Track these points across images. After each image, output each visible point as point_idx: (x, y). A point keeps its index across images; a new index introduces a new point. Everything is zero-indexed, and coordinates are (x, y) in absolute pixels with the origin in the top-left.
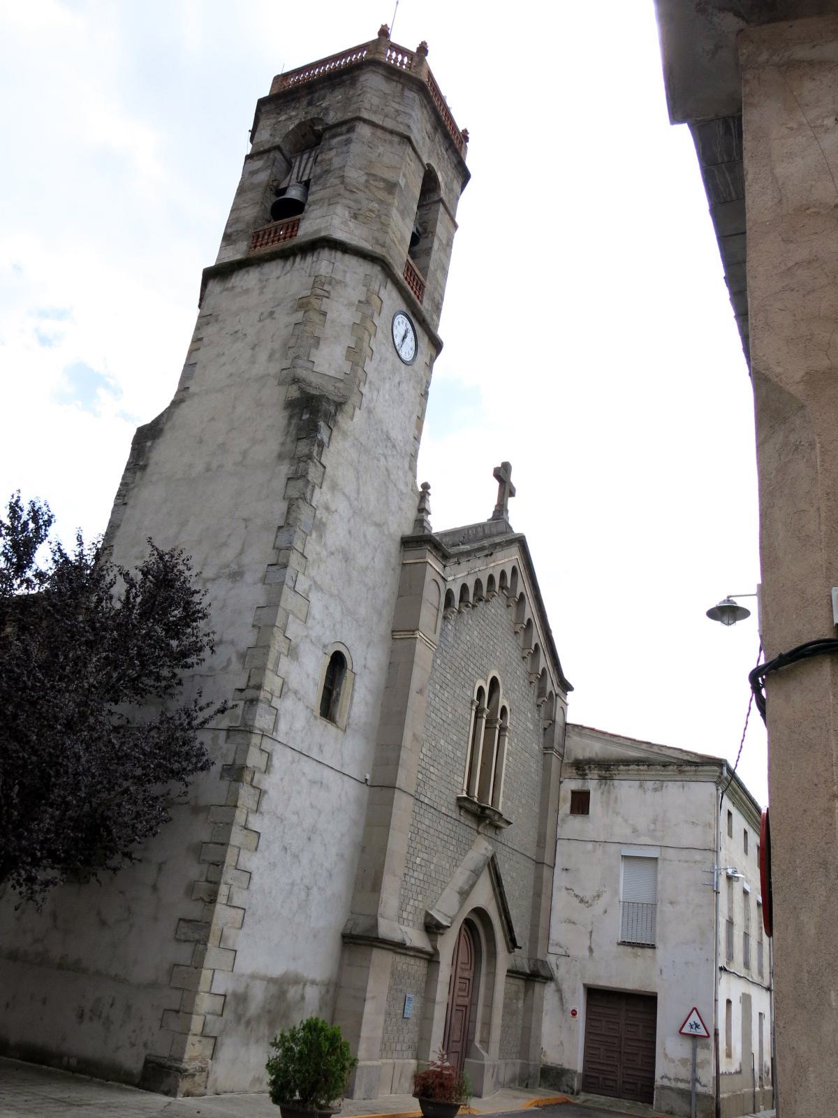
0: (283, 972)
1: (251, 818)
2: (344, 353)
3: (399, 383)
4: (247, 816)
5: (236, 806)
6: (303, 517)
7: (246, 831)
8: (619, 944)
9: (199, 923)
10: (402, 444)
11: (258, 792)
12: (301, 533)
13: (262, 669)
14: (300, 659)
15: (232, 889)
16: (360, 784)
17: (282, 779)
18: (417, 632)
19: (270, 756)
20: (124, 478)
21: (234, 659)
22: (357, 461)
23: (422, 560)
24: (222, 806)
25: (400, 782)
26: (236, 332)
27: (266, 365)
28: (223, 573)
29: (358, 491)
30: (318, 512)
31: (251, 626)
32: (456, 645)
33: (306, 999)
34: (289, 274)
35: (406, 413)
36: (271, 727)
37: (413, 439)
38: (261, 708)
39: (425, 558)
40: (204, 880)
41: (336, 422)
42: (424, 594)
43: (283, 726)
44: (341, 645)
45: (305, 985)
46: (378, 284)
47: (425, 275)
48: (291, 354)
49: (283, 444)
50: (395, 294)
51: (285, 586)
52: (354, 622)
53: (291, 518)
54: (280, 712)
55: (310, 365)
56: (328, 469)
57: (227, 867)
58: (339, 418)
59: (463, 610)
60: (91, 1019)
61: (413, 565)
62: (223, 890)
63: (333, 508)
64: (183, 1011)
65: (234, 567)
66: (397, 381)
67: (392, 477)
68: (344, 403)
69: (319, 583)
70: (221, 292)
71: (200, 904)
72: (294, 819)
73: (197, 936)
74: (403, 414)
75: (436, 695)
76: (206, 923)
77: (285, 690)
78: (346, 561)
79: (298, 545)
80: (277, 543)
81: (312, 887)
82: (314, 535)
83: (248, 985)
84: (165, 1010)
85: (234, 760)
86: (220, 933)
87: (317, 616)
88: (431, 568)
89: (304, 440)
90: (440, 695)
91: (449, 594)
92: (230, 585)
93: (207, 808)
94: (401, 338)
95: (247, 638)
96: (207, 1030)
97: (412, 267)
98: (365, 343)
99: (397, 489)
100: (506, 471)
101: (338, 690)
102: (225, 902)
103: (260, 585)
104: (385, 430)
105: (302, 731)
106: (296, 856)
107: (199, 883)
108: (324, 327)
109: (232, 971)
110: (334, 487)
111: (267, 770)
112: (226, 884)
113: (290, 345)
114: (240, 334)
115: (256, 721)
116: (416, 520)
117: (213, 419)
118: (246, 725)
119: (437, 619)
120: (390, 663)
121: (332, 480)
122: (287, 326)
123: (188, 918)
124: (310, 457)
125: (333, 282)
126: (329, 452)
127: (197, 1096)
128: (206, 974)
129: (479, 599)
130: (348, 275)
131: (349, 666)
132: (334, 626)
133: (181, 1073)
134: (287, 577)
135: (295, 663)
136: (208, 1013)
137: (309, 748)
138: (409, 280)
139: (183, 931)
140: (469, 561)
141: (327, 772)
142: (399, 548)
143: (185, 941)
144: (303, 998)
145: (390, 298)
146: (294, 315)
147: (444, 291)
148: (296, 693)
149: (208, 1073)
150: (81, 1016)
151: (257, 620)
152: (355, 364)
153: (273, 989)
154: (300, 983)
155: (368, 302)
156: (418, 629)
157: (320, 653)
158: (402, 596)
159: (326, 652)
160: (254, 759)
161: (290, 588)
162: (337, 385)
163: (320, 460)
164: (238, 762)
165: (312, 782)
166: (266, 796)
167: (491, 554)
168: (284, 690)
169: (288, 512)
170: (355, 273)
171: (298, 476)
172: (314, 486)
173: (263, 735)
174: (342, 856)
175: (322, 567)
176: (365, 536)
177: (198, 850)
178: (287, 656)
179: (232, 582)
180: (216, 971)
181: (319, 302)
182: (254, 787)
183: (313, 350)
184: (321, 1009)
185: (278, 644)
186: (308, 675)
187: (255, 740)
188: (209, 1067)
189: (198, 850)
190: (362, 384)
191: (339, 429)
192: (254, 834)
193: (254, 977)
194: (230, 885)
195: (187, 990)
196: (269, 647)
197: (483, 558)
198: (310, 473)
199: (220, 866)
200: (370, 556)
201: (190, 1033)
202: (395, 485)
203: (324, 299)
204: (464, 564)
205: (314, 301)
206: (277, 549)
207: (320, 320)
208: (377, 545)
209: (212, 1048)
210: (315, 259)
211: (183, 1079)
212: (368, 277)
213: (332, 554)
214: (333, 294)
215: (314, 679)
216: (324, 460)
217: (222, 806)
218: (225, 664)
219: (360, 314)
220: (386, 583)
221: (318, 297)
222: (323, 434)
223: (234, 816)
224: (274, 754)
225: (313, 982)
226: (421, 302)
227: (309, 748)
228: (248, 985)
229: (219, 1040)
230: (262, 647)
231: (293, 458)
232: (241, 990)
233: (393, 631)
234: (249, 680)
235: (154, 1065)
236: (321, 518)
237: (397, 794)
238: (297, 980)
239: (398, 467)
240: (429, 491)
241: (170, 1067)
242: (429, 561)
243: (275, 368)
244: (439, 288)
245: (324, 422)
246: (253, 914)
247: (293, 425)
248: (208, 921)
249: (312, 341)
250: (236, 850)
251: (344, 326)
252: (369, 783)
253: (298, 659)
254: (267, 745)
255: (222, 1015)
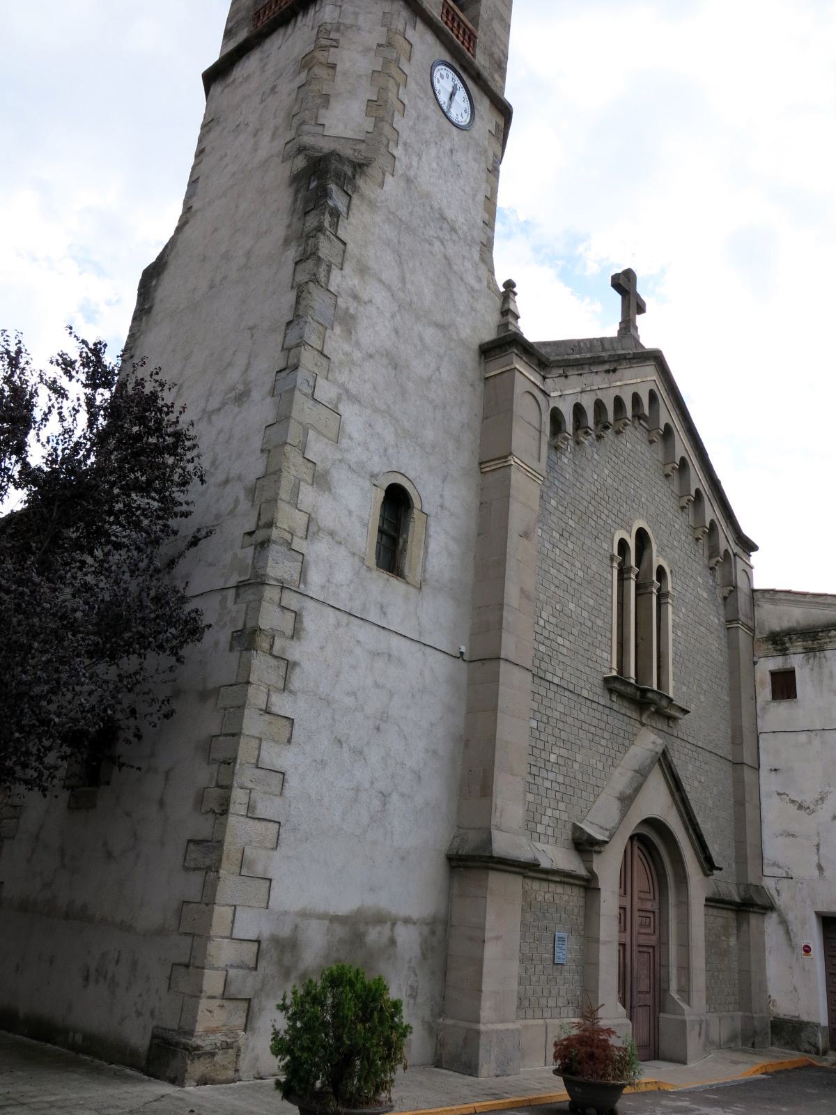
0: (355, 908)
1: (275, 698)
2: (364, 108)
3: (451, 151)
4: (268, 695)
5: (248, 683)
6: (316, 305)
7: (267, 717)
8: (415, 29)
9: (210, 844)
10: (465, 228)
11: (283, 664)
12: (315, 325)
13: (273, 501)
14: (333, 490)
15: (252, 795)
16: (453, 658)
17: (322, 648)
18: (510, 458)
19: (298, 616)
20: (131, 330)
21: (242, 497)
22: (396, 241)
23: (508, 368)
24: (231, 685)
25: (508, 649)
26: (238, 126)
27: (270, 146)
28: (229, 399)
29: (403, 280)
30: (340, 300)
31: (259, 451)
32: (578, 484)
33: (399, 943)
34: (290, 38)
35: (467, 189)
36: (296, 577)
37: (482, 224)
38: (275, 551)
39: (512, 363)
40: (213, 784)
41: (356, 188)
42: (514, 409)
43: (315, 577)
44: (399, 475)
45: (394, 924)
46: (403, 22)
47: (476, 25)
48: (295, 122)
49: (289, 226)
50: (430, 38)
51: (297, 393)
52: (418, 448)
53: (301, 307)
54: (307, 558)
55: (319, 129)
56: (350, 246)
57: (241, 764)
58: (360, 182)
59: (582, 439)
60: (97, 981)
61: (498, 377)
62: (238, 796)
63: (366, 297)
64: (193, 965)
65: (241, 387)
66: (448, 146)
67: (455, 267)
68: (367, 165)
69: (354, 393)
70: (222, 91)
71: (211, 817)
72: (349, 701)
73: (208, 862)
74: (463, 191)
75: (554, 546)
76: (218, 842)
77: (313, 528)
78: (395, 368)
79: (314, 340)
80: (286, 343)
81: (390, 795)
82: (338, 329)
83: (296, 927)
84: (174, 964)
85: (245, 624)
86: (239, 856)
87: (355, 435)
88: (522, 377)
89: (313, 212)
90: (560, 545)
91: (556, 416)
92: (236, 410)
93: (217, 691)
94: (448, 96)
95: (254, 466)
96: (232, 990)
97: (453, 10)
98: (390, 94)
99: (465, 284)
100: (629, 281)
101: (405, 536)
102: (244, 813)
103: (269, 399)
104: (436, 206)
105: (348, 586)
106: (359, 752)
107: (209, 790)
108: (334, 81)
109: (267, 908)
110: (363, 270)
111: (296, 634)
112: (241, 788)
113: (294, 113)
114: (242, 126)
115: (269, 569)
116: (499, 326)
117: (216, 230)
118: (257, 576)
119: (540, 445)
120: (481, 504)
121: (359, 261)
122: (290, 95)
123: (196, 838)
124: (320, 229)
125: (342, 28)
126: (349, 224)
127: (221, 1083)
128: (221, 913)
129: (604, 426)
130: (361, 18)
131: (416, 504)
132: (386, 450)
133: (190, 1053)
134: (299, 381)
135: (326, 495)
136: (232, 966)
137: (364, 608)
138: (462, 39)
139: (193, 856)
140: (581, 375)
141: (396, 641)
142: (477, 358)
143: (195, 869)
144: (393, 942)
145: (424, 44)
146: (298, 78)
147: (506, 46)
148: (332, 534)
149: (239, 1050)
150: (87, 978)
151: (267, 442)
152: (379, 120)
153: (340, 931)
154: (386, 922)
155: (390, 44)
156: (511, 454)
157: (367, 485)
158: (487, 418)
159: (376, 483)
160: (270, 618)
161: (305, 395)
162: (357, 147)
163: (336, 233)
164: (250, 624)
165: (375, 654)
166: (297, 670)
167: (614, 371)
168: (312, 528)
169: (297, 302)
170: (370, 13)
171: (308, 256)
172: (329, 266)
173: (283, 588)
174: (435, 752)
175: (357, 372)
176: (421, 339)
177: (206, 748)
178: (312, 484)
179: (239, 406)
180: (238, 908)
181: (325, 54)
182: (276, 657)
183: (322, 111)
184: (424, 956)
185: (294, 467)
186: (350, 513)
187: (270, 593)
188: (241, 1042)
189: (206, 748)
190: (391, 144)
191: (362, 197)
192: (284, 722)
193: (305, 915)
194: (250, 790)
195: (198, 936)
196: (280, 470)
197: (604, 375)
198: (320, 247)
199: (231, 765)
200: (433, 366)
201: (203, 995)
202: (462, 279)
203: (332, 50)
204: (574, 379)
205: (319, 55)
206: (286, 350)
207: (329, 75)
208: (442, 352)
209: (244, 1015)
210: (317, 8)
211: (192, 1061)
212: (388, 16)
213: (371, 356)
214: (342, 41)
215: (361, 519)
216: (341, 233)
217: (231, 685)
218: (232, 506)
219: (381, 59)
220: (463, 402)
221: (324, 48)
222: (337, 199)
223: (247, 695)
224: (304, 613)
225: (407, 921)
226: (474, 56)
227: (364, 608)
228: (296, 927)
229: (255, 1003)
230: (273, 474)
231: (301, 237)
232: (285, 932)
233: (480, 464)
234: (259, 519)
235: (160, 1040)
236: (347, 309)
237: (503, 666)
238: (380, 919)
239: (464, 257)
240: (515, 289)
241: (177, 1044)
242: (518, 366)
243: (279, 144)
244: (498, 42)
245: (337, 184)
246: (295, 829)
247: (299, 200)
248: (220, 839)
249: (319, 101)
250: (255, 743)
251: (360, 76)
252: (466, 657)
253: (330, 490)
254: (291, 600)
255: (256, 969)
